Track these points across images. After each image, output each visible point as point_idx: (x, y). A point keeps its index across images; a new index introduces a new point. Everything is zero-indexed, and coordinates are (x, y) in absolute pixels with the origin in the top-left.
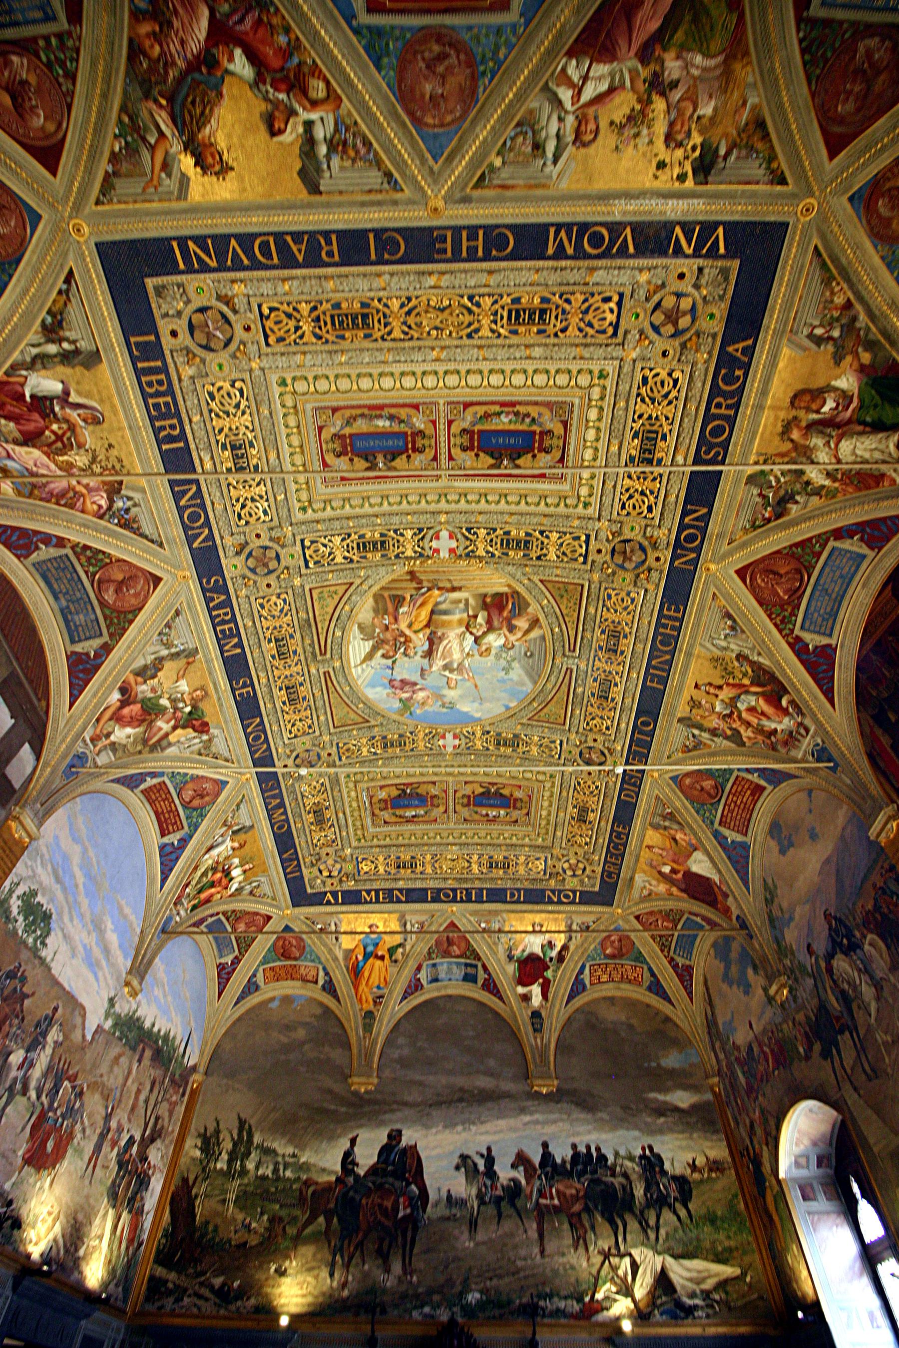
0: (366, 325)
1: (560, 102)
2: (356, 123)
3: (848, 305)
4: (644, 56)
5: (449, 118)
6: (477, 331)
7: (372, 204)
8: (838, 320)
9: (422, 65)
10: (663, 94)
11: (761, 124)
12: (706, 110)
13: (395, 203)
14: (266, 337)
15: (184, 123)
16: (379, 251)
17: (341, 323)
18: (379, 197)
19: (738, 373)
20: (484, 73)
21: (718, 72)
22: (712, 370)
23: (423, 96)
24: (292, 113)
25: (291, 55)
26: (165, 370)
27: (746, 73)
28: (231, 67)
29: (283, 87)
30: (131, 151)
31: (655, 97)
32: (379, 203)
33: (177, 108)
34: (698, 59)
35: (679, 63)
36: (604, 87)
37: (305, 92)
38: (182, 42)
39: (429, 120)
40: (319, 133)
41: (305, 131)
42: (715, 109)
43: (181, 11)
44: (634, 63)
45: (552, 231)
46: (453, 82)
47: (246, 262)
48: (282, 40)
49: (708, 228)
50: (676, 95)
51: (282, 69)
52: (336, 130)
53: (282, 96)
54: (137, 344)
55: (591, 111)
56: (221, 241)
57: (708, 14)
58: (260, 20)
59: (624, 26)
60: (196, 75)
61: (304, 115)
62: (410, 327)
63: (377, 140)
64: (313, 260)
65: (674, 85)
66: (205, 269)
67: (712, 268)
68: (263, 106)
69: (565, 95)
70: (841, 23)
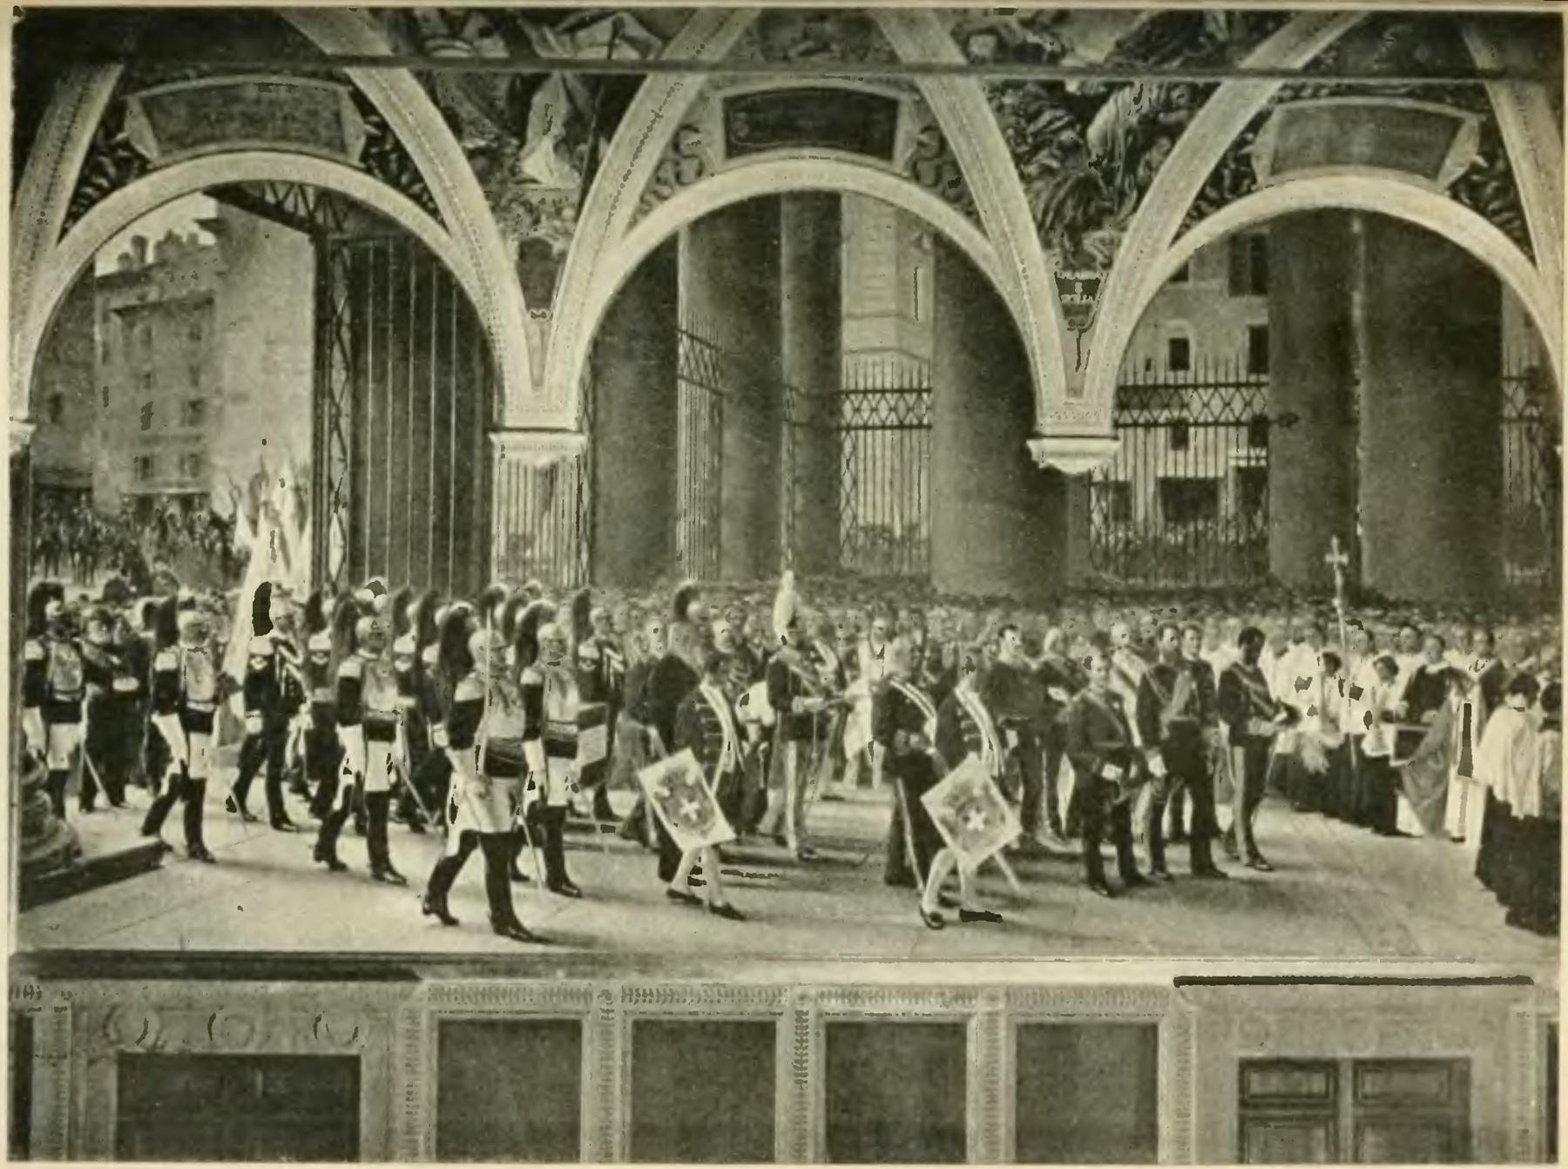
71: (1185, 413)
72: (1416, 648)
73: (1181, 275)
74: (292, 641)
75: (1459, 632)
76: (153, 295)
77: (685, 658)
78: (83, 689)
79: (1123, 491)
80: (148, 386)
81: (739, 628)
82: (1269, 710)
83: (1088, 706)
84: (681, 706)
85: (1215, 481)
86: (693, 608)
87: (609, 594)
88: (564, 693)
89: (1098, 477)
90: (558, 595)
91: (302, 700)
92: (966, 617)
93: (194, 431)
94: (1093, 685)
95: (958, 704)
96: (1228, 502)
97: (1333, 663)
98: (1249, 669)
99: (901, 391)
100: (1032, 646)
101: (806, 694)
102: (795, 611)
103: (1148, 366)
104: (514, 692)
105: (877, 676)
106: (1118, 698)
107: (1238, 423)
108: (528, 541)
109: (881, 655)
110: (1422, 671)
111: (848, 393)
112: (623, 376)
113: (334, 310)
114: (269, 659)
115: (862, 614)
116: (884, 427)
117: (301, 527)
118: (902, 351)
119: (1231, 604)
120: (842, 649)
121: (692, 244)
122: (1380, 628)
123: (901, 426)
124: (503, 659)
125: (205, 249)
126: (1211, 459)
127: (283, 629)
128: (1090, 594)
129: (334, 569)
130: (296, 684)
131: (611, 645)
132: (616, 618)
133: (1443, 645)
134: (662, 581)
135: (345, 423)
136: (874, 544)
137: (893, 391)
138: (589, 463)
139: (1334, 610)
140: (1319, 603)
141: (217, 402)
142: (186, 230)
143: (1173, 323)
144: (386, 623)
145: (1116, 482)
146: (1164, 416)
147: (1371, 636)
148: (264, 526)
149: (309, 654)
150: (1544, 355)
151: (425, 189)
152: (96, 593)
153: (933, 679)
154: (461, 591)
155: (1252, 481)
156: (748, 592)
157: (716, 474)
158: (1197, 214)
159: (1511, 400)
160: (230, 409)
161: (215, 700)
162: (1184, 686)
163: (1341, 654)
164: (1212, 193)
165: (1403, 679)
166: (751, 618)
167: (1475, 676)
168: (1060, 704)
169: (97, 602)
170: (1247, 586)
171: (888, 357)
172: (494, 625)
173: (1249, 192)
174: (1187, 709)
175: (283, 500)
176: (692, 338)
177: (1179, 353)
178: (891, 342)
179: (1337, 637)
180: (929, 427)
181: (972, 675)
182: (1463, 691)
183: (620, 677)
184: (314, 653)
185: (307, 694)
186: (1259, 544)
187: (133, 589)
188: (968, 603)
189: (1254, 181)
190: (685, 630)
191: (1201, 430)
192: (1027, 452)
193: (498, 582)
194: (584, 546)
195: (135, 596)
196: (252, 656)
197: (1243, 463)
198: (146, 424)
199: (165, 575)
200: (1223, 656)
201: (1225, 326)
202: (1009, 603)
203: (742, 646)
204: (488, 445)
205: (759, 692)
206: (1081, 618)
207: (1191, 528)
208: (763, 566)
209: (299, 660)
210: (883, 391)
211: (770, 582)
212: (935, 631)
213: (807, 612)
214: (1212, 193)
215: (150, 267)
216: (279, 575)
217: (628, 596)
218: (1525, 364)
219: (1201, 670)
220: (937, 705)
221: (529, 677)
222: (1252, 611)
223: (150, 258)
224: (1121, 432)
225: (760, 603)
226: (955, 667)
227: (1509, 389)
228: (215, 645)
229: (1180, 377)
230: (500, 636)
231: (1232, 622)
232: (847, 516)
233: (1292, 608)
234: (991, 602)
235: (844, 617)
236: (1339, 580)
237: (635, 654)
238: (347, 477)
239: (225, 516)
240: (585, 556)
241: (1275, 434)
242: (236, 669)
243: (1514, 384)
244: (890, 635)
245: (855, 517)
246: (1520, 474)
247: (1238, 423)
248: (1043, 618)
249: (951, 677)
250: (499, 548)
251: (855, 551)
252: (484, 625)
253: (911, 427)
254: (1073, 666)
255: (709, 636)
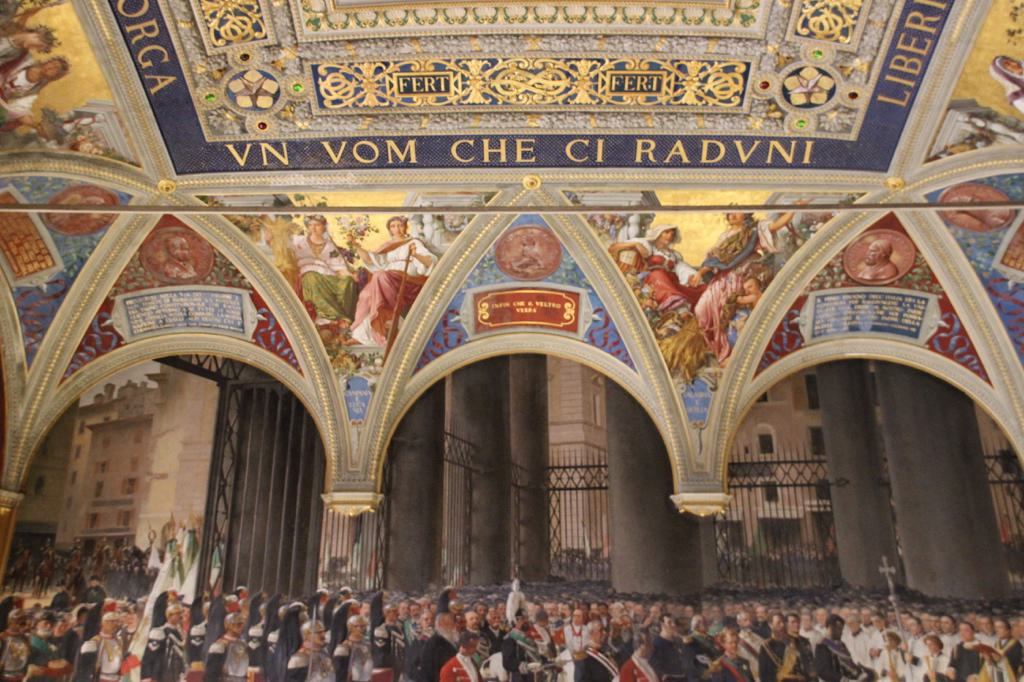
0: (621, 80)
1: (425, 245)
2: (600, 235)
3: (74, 147)
4: (365, 277)
5: (519, 233)
6: (485, 68)
7: (595, 184)
8: (75, 135)
9: (540, 262)
10: (340, 249)
11: (246, 230)
12: (297, 239)
13: (571, 184)
14: (745, 75)
15: (749, 238)
16: (591, 151)
17: (650, 82)
18: (586, 189)
19: (149, 64)
20: (490, 260)
21: (301, 262)
22: (179, 52)
23: (541, 245)
24: (653, 243)
25: (643, 280)
26: (885, 69)
27: (277, 262)
28: (694, 272)
29: (655, 259)
30: (808, 223)
31: (347, 248)
32: (587, 184)
33: (751, 247)
34: (321, 271)
35: (336, 268)
36: (391, 255)
37: (639, 256)
38: (724, 289)
39: (536, 231)
40: (633, 229)
41: (645, 231)
42: (291, 240)
43: (716, 310)
44: (371, 270)
45: (413, 160)
46: (515, 252)
47: (738, 144)
48: (647, 290)
49: (254, 164)
50: (329, 248)
51: (652, 270)
52: (617, 231)
53: (658, 253)
54: (902, 98)
55: (397, 239)
56: (756, 162)
57: (326, 299)
58: (659, 302)
59: (388, 295)
60: (723, 267)
61: (644, 241)
62: (568, 75)
63: (582, 223)
64: (664, 143)
65: (333, 254)
66: (785, 142)
67: (232, 133)
68: (676, 247)
69: (421, 250)
70: (219, 284)
71: (773, 479)
72: (954, 631)
73: (764, 398)
74: (180, 630)
75: (983, 620)
76: (114, 416)
77: (446, 636)
78: (25, 671)
79: (737, 527)
80: (103, 471)
81: (484, 616)
82: (855, 673)
83: (725, 668)
84: (443, 669)
85: (798, 520)
86: (452, 603)
87: (396, 596)
88: (363, 664)
89: (719, 518)
90: (362, 596)
91: (181, 669)
92: (635, 609)
93: (129, 497)
94: (727, 653)
95: (635, 666)
96: (809, 533)
97: (895, 640)
98: (836, 642)
99: (588, 467)
100: (681, 625)
101: (529, 660)
102: (520, 602)
103: (747, 451)
104: (329, 662)
105: (577, 647)
106: (747, 662)
107: (809, 485)
108: (344, 562)
109: (580, 634)
110: (960, 647)
111: (553, 468)
112: (410, 461)
113: (228, 422)
114: (162, 643)
115: (566, 606)
116: (577, 489)
117: (194, 556)
118: (586, 443)
119: (817, 599)
120: (553, 630)
121: (454, 384)
122: (925, 617)
123: (588, 488)
124: (323, 639)
125: (151, 390)
126: (794, 507)
127: (174, 623)
128: (718, 594)
129: (212, 581)
130: (180, 659)
131: (396, 629)
132: (401, 611)
133: (974, 629)
134: (433, 586)
135: (229, 491)
136: (573, 561)
137: (582, 467)
138: (384, 510)
139: (890, 604)
140: (879, 599)
141: (147, 479)
142: (138, 378)
143: (760, 425)
144: (245, 615)
145: (732, 522)
146: (760, 480)
147: (919, 621)
148: (168, 557)
149: (190, 638)
150: (1009, 444)
151: (292, 352)
152: (46, 602)
153: (616, 650)
154: (297, 595)
155: (822, 520)
156: (491, 593)
157: (468, 518)
158: (768, 359)
159: (992, 470)
160: (156, 484)
161: (119, 673)
162: (791, 657)
163: (899, 633)
164: (777, 347)
165: (947, 651)
166: (491, 609)
167: (1001, 652)
168: (706, 666)
169: (46, 608)
170: (828, 588)
171: (578, 447)
172: (318, 618)
173: (800, 347)
174: (796, 670)
175: (183, 540)
176: (453, 436)
177: (766, 443)
178: (583, 439)
179: (895, 621)
180: (606, 488)
181: (643, 647)
182: (994, 663)
183: (402, 651)
184: (194, 637)
185: (186, 665)
186: (833, 559)
187: (74, 598)
188: (637, 598)
189: (803, 341)
190: (447, 617)
191: (785, 489)
192: (670, 505)
193: (322, 587)
194: (380, 565)
195: (74, 604)
196: (150, 641)
197: (815, 509)
198: (98, 494)
199: (97, 588)
200: (815, 633)
201: (793, 427)
202: (665, 598)
203: (484, 628)
204: (321, 503)
205: (497, 661)
206: (715, 608)
207: (785, 550)
208: (500, 577)
209: (183, 644)
210: (576, 467)
211: (505, 586)
212: (616, 619)
213: (531, 609)
214: (777, 347)
215: (116, 400)
216: (174, 586)
217: (409, 594)
218: (998, 448)
219: (801, 643)
220: (620, 666)
221: (339, 651)
222: (833, 604)
223: (115, 395)
224: (732, 490)
225: (498, 600)
226: (631, 640)
227: (990, 463)
228: (125, 634)
229: (768, 457)
230: (321, 624)
231: (821, 612)
232: (554, 543)
233: (862, 604)
234: (654, 598)
235: (556, 609)
236: (891, 584)
237: (411, 633)
238: (227, 522)
239: (143, 549)
240: (380, 571)
241: (833, 490)
242: (137, 649)
243: (992, 461)
244: (586, 621)
245: (560, 544)
246: (1008, 516)
247: (809, 485)
248: (689, 608)
249: (629, 649)
250: (324, 566)
251: (560, 566)
252: (311, 617)
253: (595, 488)
254: (712, 640)
255: (463, 622)
